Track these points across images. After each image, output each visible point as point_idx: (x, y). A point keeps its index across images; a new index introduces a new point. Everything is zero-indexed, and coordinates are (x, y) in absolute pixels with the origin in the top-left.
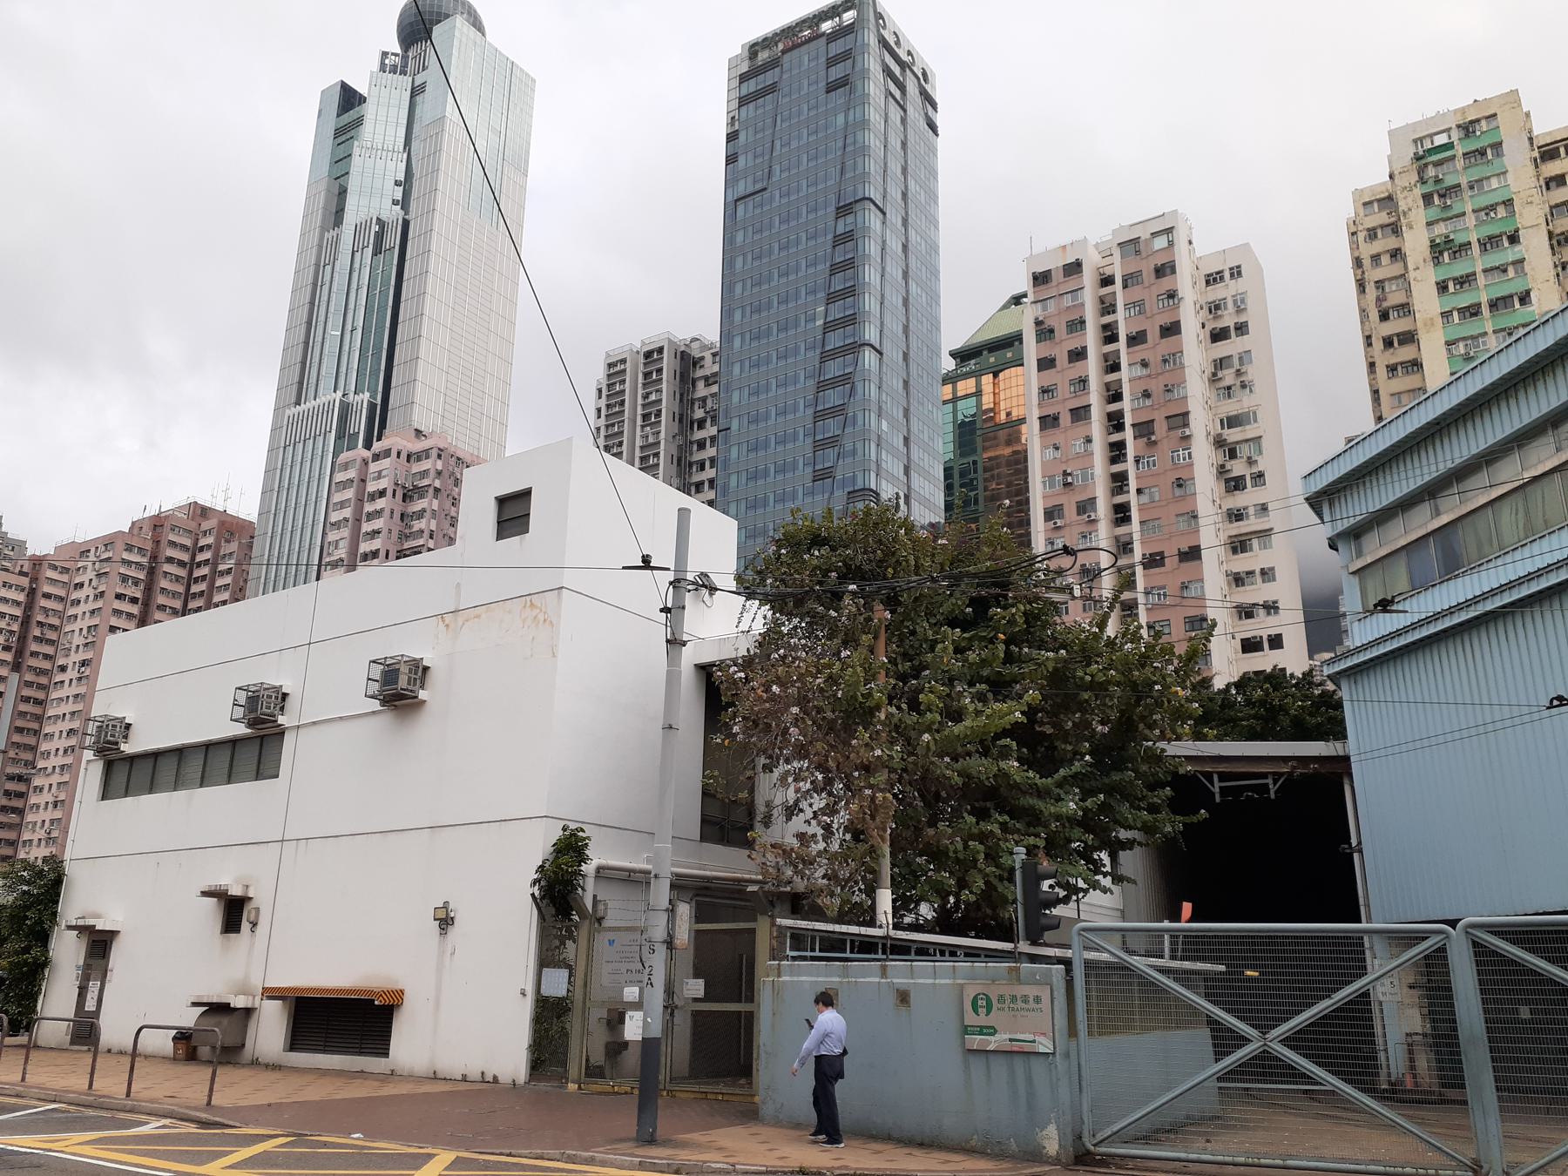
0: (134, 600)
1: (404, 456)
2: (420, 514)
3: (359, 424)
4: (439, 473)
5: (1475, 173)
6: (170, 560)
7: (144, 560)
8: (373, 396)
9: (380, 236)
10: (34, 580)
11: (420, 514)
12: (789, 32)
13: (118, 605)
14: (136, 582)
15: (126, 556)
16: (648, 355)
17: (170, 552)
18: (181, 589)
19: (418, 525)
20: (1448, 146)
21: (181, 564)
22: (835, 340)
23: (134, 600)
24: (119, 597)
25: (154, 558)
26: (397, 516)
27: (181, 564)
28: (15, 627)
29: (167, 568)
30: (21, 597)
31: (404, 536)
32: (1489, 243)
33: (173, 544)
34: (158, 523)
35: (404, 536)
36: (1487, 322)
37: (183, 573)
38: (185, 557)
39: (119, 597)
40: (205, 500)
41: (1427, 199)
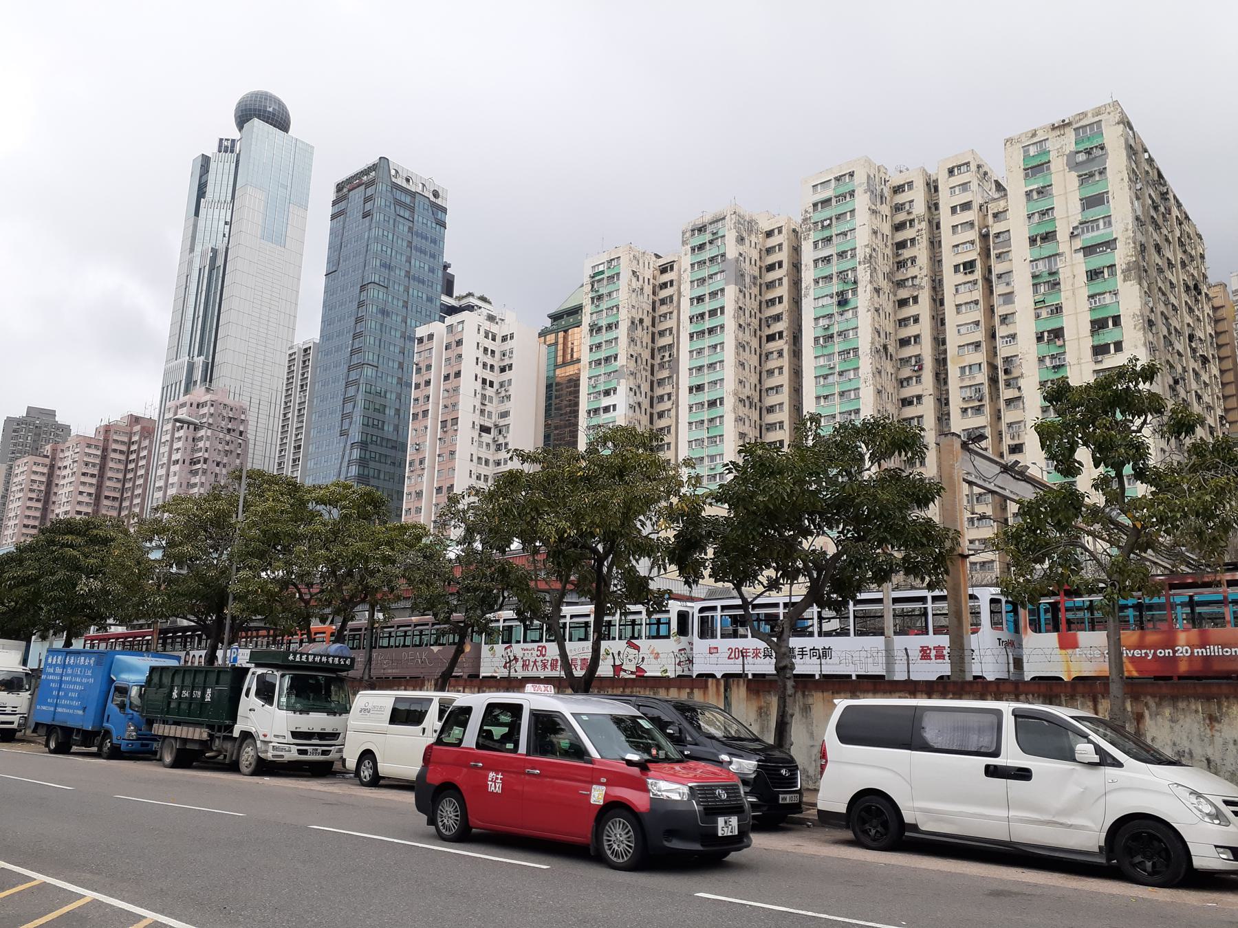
0: (93, 476)
1: (195, 405)
2: (201, 438)
3: (198, 375)
4: (212, 415)
5: (611, 288)
6: (115, 451)
7: (99, 453)
8: (207, 358)
9: (213, 259)
10: (53, 459)
11: (201, 438)
12: (349, 180)
13: (83, 479)
14: (94, 465)
15: (87, 450)
16: (305, 350)
17: (115, 446)
18: (122, 467)
19: (201, 444)
20: (602, 272)
21: (121, 452)
22: (355, 361)
23: (93, 476)
24: (84, 474)
25: (105, 450)
26: (190, 439)
27: (121, 452)
28: (43, 488)
29: (113, 455)
30: (45, 470)
31: (194, 451)
32: (609, 327)
33: (116, 441)
34: (107, 429)
35: (194, 451)
36: (602, 369)
37: (123, 457)
38: (124, 448)
39: (84, 474)
40: (139, 413)
41: (592, 299)
